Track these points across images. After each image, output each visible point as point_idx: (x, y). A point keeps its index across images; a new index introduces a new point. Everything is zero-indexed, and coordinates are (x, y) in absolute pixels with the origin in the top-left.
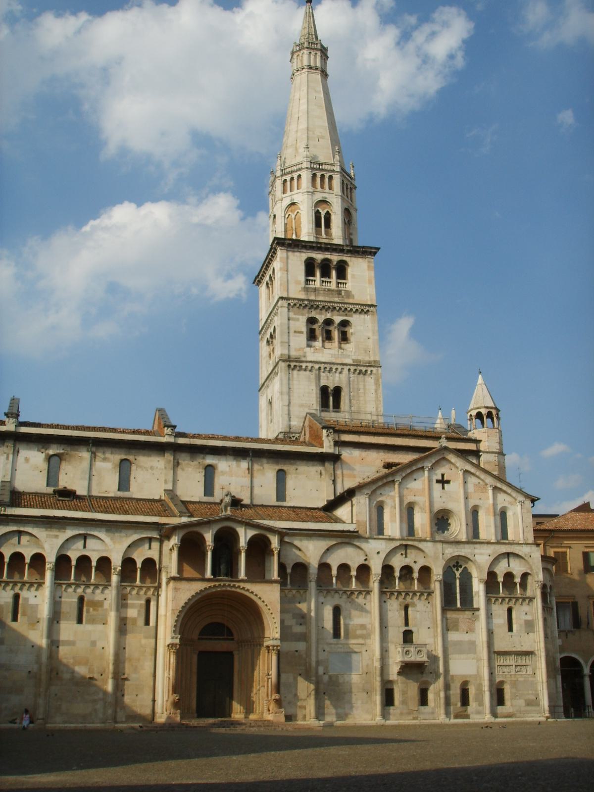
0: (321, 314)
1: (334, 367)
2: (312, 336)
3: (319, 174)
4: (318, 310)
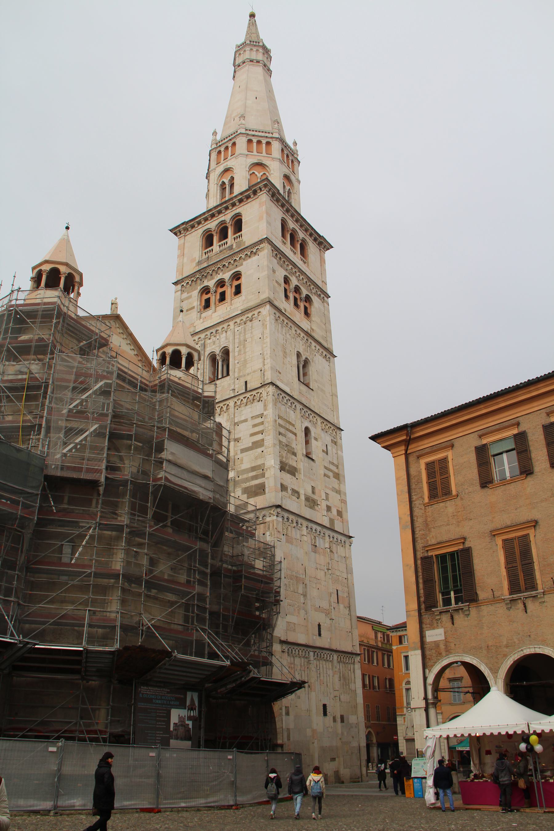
0: (213, 279)
1: (220, 328)
2: (207, 305)
3: (222, 149)
4: (209, 277)
